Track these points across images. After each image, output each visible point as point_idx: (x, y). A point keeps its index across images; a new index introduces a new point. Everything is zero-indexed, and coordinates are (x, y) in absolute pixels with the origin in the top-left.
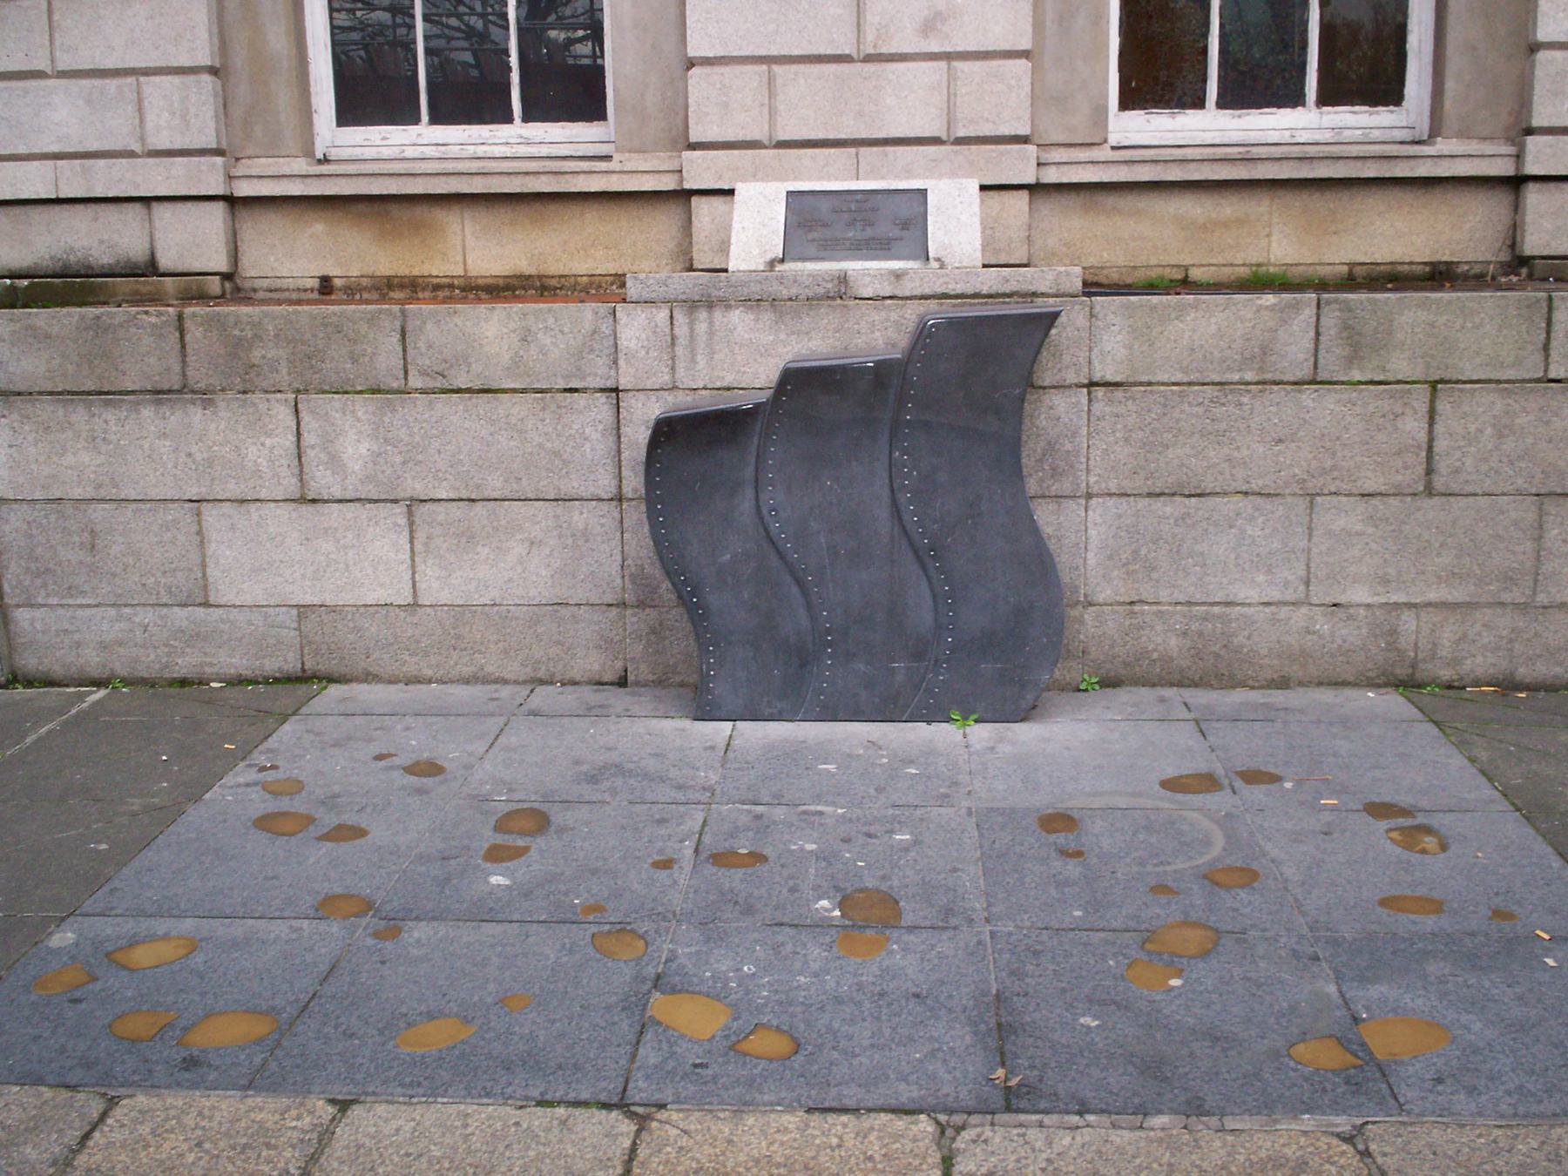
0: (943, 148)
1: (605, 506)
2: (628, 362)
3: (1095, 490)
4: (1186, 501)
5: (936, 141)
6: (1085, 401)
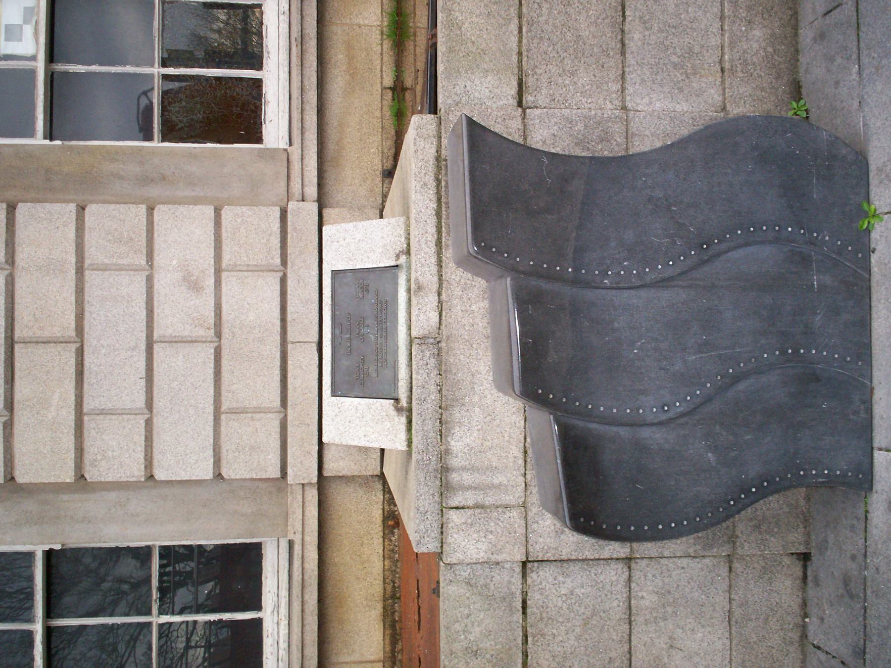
0: (289, 275)
1: (636, 575)
2: (500, 551)
3: (618, 103)
4: (628, 19)
5: (283, 281)
6: (537, 112)
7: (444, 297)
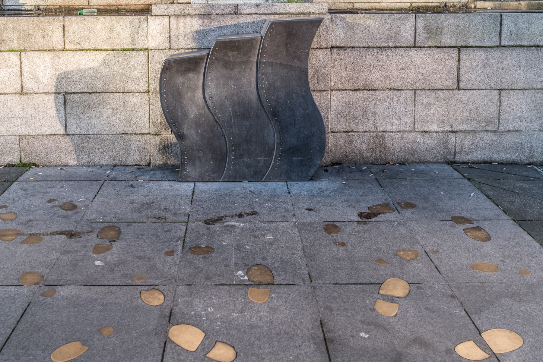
1: (142, 95)
2: (152, 38)
3: (334, 88)
4: (368, 92)
6: (329, 53)
7: (254, 15)
